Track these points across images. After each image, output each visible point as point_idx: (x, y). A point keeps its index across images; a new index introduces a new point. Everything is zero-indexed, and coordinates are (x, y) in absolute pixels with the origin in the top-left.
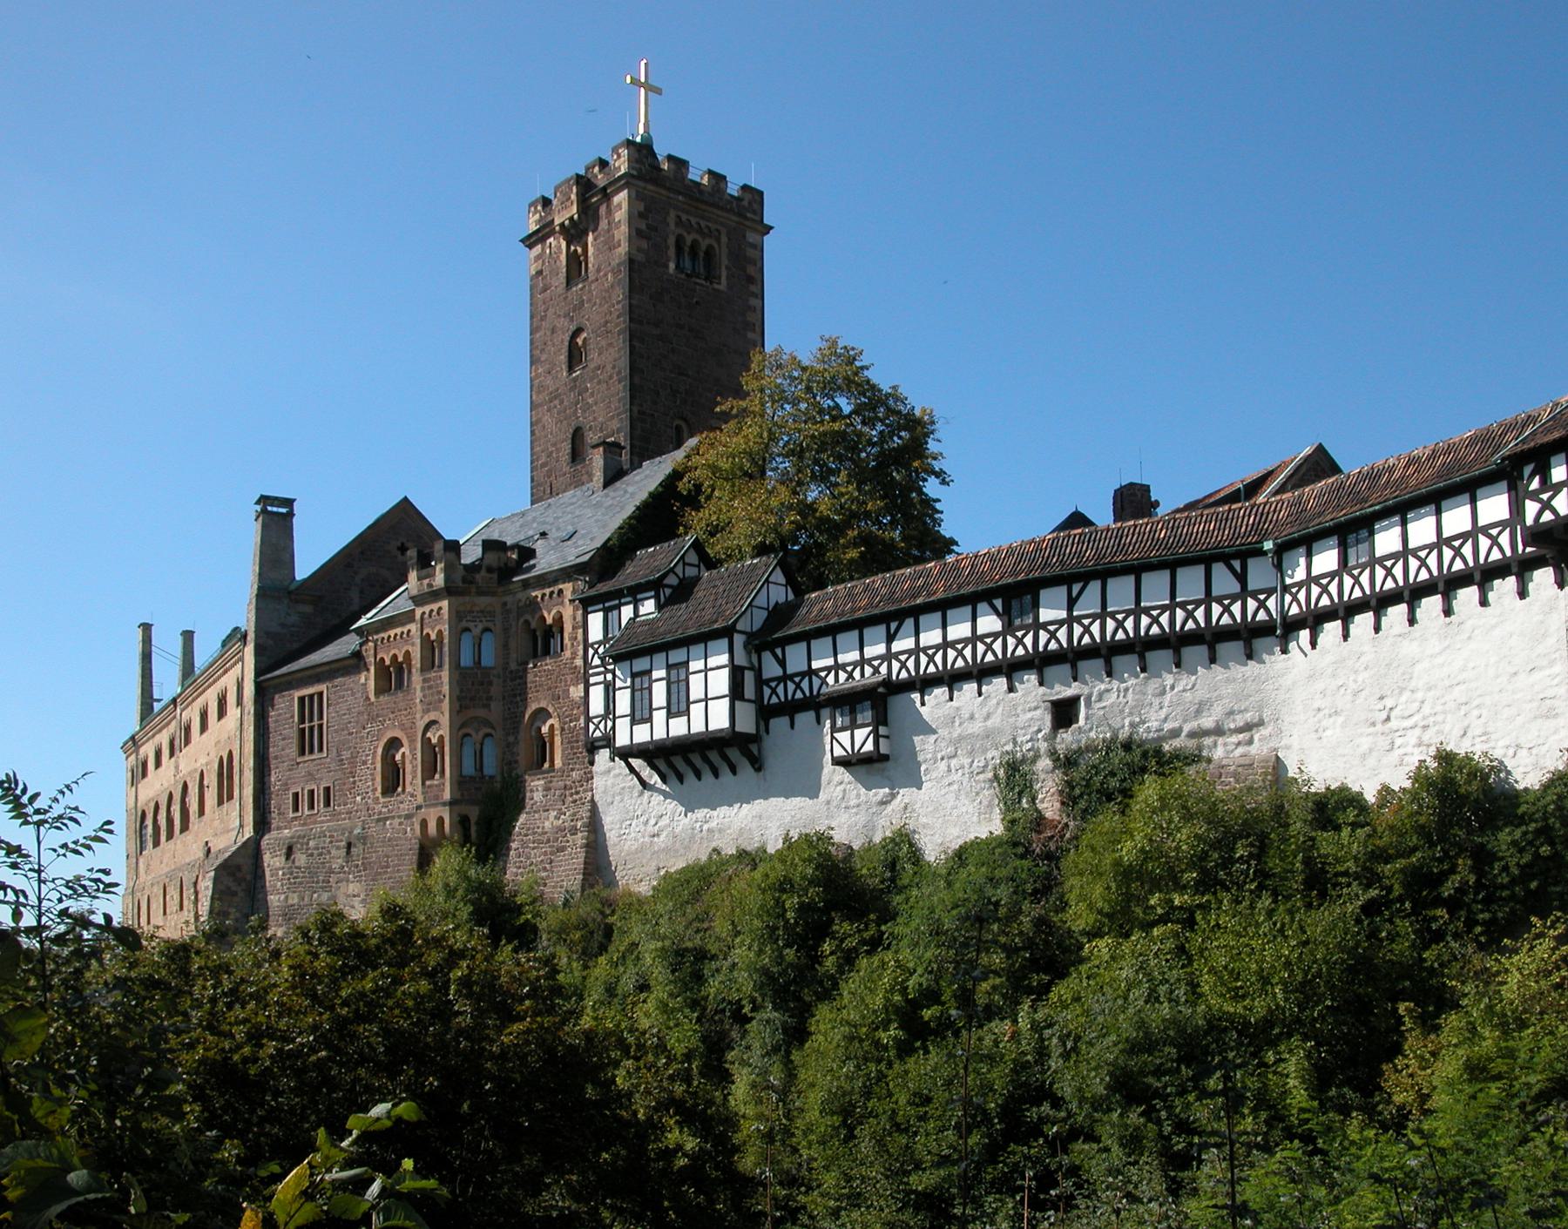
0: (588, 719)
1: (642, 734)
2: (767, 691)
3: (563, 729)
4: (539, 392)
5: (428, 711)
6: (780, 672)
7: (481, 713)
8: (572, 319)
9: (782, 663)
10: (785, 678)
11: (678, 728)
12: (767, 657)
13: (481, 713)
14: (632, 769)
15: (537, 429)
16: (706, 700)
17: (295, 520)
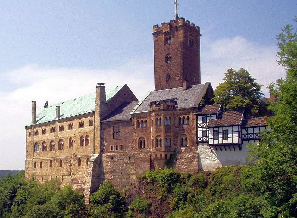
0: (197, 137)
1: (216, 142)
2: (243, 136)
3: (190, 139)
4: (157, 65)
5: (157, 133)
6: (247, 133)
7: (169, 134)
8: (166, 52)
9: (247, 131)
10: (248, 134)
11: (225, 142)
12: (244, 130)
13: (169, 134)
14: (211, 148)
15: (156, 72)
16: (232, 137)
17: (106, 88)
